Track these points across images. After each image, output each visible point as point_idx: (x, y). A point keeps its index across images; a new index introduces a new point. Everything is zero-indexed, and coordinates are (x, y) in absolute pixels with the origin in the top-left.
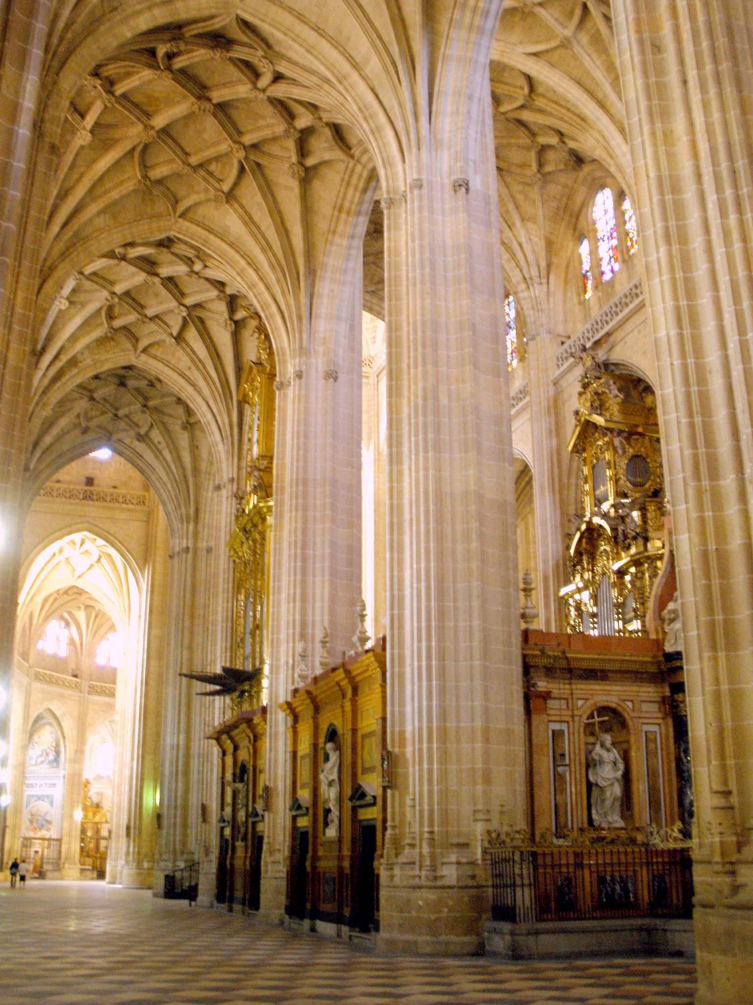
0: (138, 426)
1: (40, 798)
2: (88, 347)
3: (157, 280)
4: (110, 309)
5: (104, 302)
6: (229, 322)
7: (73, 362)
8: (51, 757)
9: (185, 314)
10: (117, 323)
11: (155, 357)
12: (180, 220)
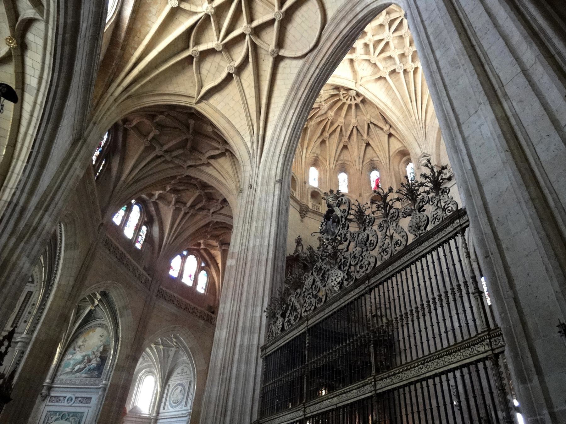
8: (94, 363)
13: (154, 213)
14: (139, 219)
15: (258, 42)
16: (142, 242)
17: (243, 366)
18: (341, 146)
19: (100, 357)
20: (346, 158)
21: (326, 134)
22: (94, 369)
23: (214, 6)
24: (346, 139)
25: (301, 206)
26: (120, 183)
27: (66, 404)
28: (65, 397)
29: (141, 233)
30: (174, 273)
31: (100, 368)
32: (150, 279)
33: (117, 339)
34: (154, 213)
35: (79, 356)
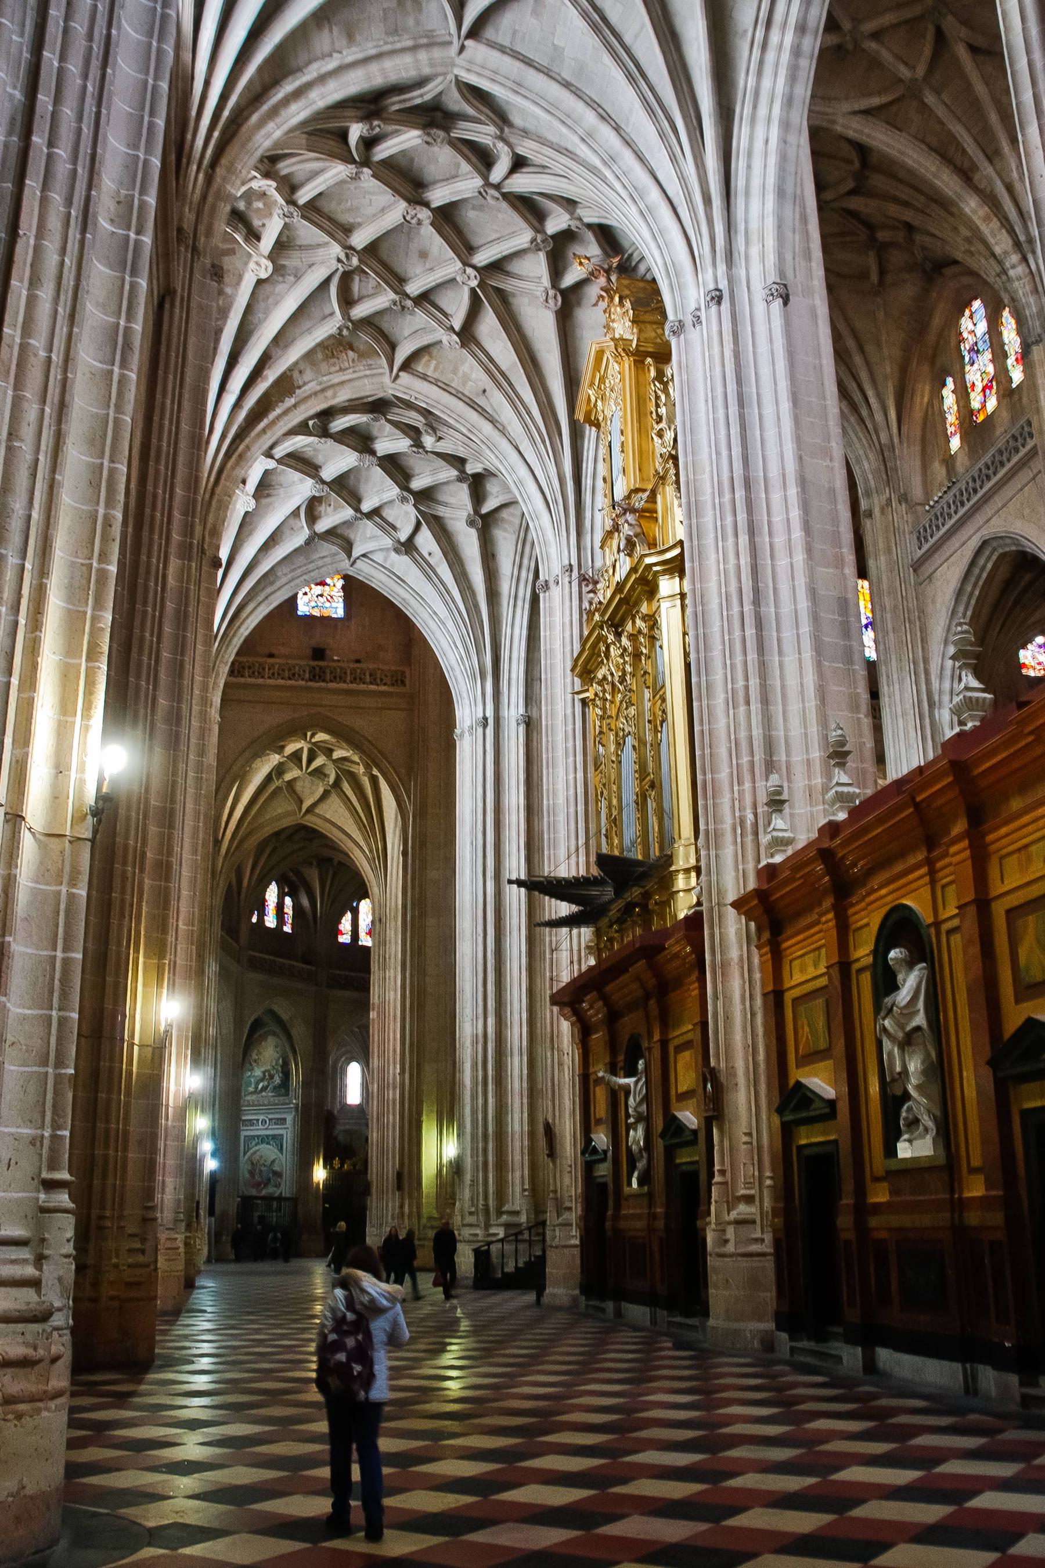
0: (394, 528)
1: (264, 1140)
2: (309, 356)
3: (424, 214)
4: (346, 278)
5: (334, 265)
6: (551, 292)
7: (285, 385)
8: (277, 1080)
9: (474, 283)
10: (360, 311)
11: (424, 377)
12: (469, 43)
13: (294, 878)
14: (278, 895)
15: (347, 766)
16: (290, 921)
17: (391, 1117)
19: (283, 1072)
22: (279, 1087)
26: (244, 891)
27: (261, 1127)
28: (258, 1120)
29: (286, 910)
30: (345, 939)
31: (284, 1086)
32: (313, 968)
33: (294, 1052)
34: (294, 878)
35: (258, 1073)
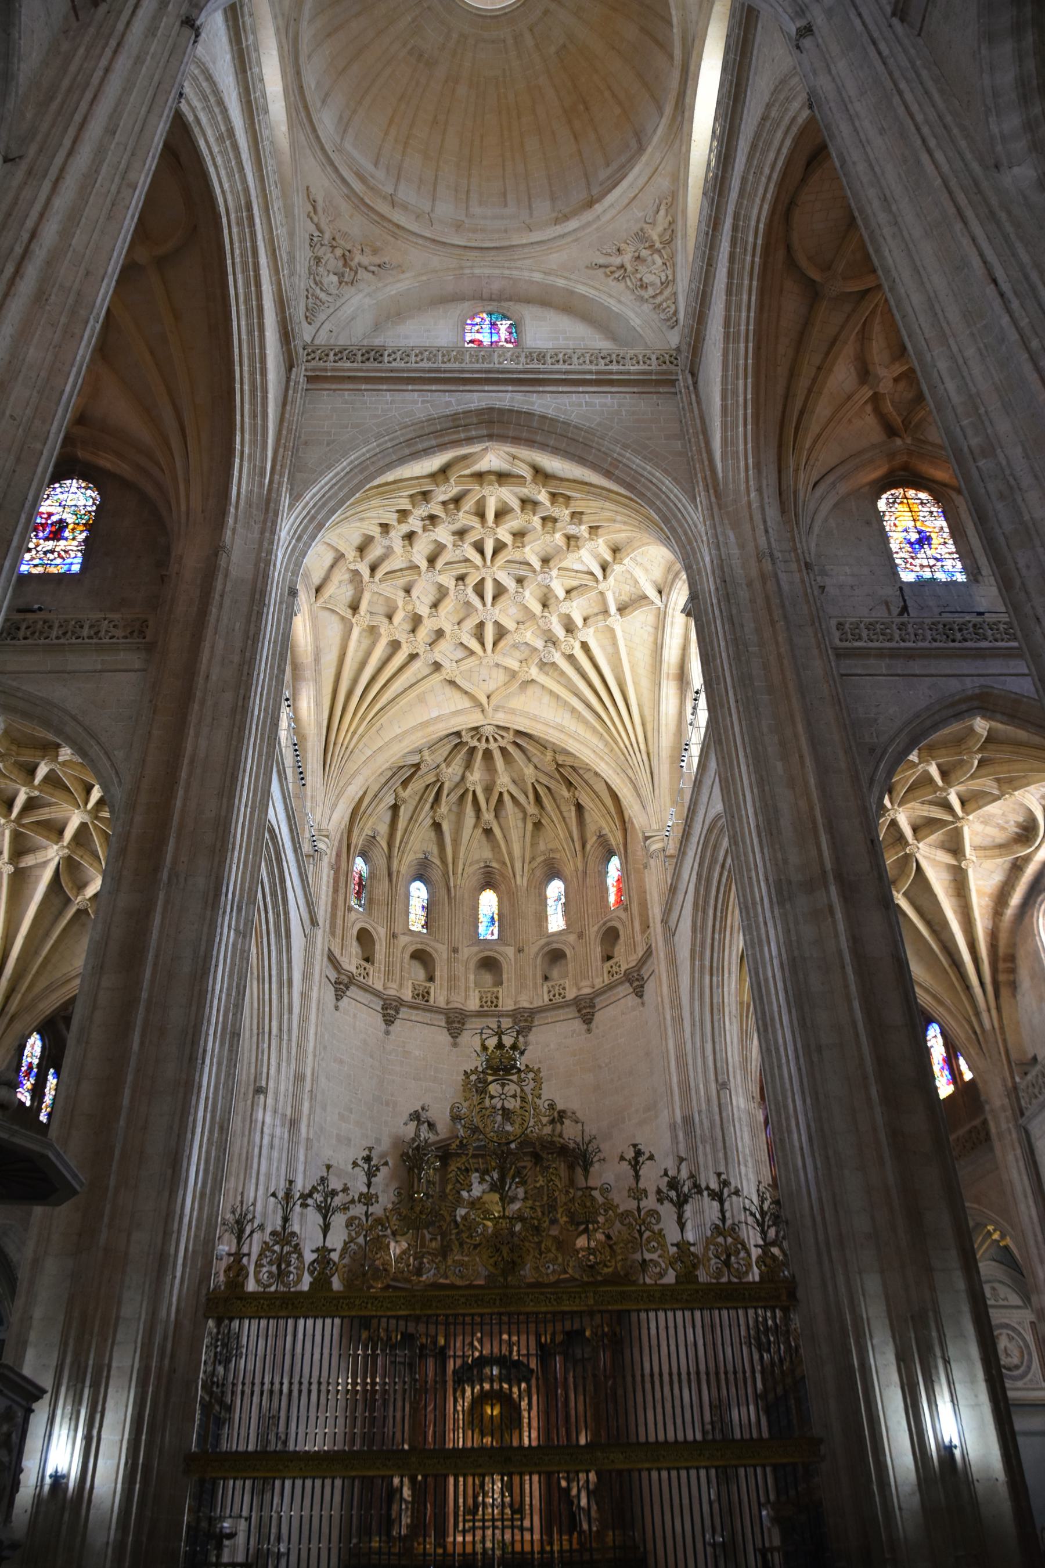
18: (530, 826)
20: (550, 846)
21: (488, 816)
23: (65, 844)
24: (532, 809)
25: (446, 1014)
